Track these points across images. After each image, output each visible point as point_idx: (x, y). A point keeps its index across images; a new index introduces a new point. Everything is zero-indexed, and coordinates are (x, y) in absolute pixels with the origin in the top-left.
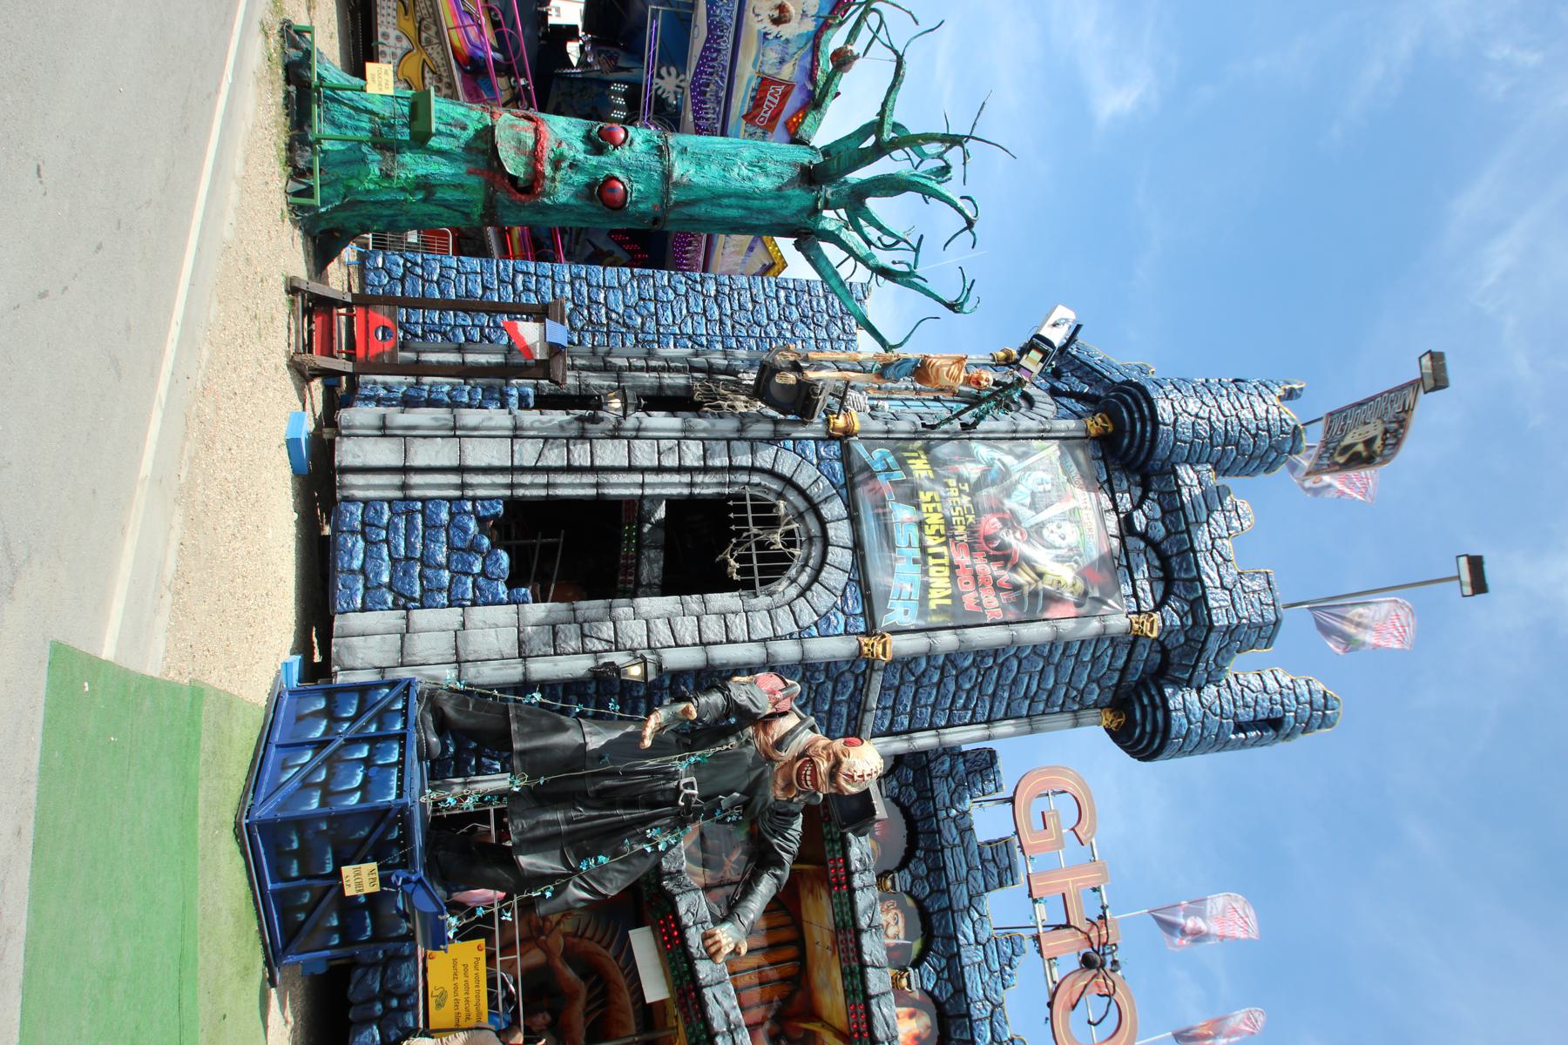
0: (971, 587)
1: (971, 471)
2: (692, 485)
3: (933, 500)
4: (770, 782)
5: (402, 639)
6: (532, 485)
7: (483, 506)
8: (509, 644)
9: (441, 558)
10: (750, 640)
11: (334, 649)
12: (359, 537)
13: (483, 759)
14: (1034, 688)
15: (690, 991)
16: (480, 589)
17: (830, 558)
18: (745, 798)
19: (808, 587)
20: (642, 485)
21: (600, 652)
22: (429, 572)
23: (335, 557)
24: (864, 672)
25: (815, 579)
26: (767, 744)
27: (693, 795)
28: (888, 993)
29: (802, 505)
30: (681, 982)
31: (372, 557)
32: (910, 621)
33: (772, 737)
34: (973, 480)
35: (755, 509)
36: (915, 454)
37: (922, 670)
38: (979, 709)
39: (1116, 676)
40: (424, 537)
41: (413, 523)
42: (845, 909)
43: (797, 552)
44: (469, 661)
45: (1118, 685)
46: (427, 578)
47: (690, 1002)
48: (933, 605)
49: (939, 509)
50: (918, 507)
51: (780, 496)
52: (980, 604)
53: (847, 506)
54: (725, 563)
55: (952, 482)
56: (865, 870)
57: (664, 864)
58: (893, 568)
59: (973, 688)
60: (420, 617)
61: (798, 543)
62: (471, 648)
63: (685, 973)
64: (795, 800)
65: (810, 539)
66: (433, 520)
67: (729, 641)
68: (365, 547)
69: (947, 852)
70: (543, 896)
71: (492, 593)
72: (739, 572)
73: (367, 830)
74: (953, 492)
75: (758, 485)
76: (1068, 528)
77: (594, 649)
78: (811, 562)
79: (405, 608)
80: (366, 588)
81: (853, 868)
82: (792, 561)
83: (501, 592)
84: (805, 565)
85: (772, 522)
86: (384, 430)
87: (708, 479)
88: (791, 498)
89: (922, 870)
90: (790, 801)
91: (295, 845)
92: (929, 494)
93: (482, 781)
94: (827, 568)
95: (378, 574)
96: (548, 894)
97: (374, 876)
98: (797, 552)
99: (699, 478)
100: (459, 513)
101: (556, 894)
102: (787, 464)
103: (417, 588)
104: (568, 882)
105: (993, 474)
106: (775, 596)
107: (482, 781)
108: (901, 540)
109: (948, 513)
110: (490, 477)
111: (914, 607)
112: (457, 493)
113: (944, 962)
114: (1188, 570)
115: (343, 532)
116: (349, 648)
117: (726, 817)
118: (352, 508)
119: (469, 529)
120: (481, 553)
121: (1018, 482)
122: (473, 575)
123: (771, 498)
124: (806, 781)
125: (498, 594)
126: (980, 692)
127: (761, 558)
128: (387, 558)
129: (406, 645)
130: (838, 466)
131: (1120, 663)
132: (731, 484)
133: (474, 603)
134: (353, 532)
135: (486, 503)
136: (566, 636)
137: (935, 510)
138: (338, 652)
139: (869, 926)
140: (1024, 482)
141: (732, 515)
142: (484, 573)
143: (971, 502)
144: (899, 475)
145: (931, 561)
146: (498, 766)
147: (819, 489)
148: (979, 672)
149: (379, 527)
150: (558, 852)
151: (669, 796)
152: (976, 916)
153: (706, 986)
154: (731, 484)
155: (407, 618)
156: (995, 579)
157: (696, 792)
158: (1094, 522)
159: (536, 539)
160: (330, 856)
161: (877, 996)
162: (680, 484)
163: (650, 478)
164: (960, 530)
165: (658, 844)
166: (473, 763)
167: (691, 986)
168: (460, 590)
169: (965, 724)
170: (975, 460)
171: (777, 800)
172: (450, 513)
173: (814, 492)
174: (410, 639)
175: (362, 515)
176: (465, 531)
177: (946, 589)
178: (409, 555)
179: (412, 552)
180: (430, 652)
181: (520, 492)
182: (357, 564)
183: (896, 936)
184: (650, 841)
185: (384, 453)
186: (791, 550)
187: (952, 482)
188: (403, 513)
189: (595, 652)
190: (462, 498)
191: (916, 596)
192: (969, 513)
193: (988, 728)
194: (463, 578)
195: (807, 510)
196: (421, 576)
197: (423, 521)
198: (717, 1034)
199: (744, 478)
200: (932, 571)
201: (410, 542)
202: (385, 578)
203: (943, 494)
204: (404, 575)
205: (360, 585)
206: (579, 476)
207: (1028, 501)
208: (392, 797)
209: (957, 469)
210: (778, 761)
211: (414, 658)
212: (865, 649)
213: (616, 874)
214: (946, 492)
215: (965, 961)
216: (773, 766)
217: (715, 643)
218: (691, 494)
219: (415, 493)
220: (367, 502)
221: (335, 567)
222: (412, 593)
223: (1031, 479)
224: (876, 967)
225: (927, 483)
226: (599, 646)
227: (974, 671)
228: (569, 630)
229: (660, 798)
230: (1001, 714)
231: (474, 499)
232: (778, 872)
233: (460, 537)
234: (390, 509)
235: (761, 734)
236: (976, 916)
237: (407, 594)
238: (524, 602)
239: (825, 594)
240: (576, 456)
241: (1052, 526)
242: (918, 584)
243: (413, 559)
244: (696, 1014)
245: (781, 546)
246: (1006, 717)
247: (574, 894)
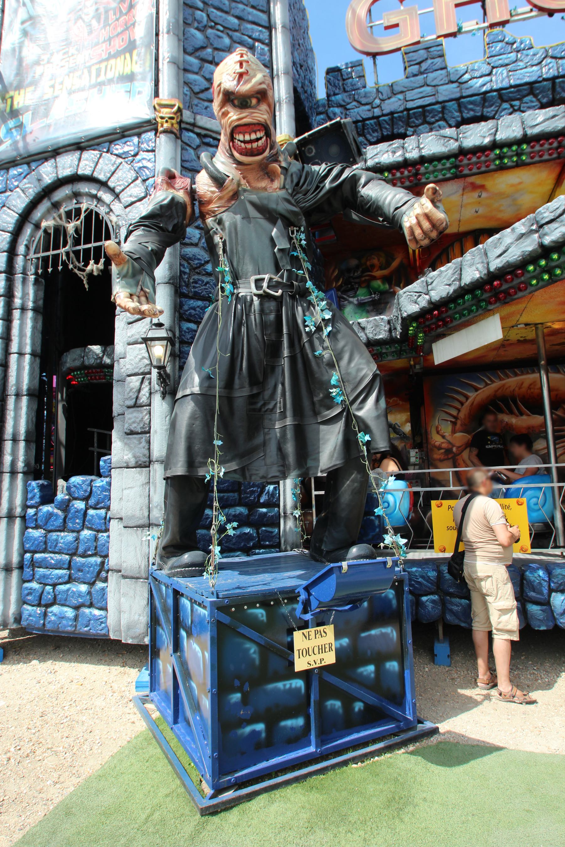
2: (23, 309)
4: (264, 194)
5: (124, 577)
6: (14, 453)
7: (32, 499)
8: (137, 476)
9: (69, 537)
11: (130, 641)
12: (49, 610)
13: (262, 500)
15: (493, 288)
16: (98, 503)
17: (88, 172)
18: (279, 222)
19: (112, 190)
20: (21, 354)
21: (150, 389)
22: (81, 550)
23: (63, 632)
24: (198, 135)
25: (103, 184)
26: (220, 198)
27: (271, 279)
28: (522, 118)
29: (45, 205)
30: (483, 300)
31: (66, 600)
33: (213, 192)
35: (46, 249)
37: (202, 80)
38: (256, 35)
40: (54, 553)
41: (41, 562)
42: (440, 167)
43: (84, 207)
44: (149, 515)
46: (85, 551)
47: (505, 287)
51: (37, 226)
53: (46, 159)
54: (90, 275)
56: (403, 148)
57: (381, 337)
59: (230, 37)
60: (113, 561)
61: (77, 206)
62: (138, 513)
63: (474, 297)
64: (284, 164)
65: (76, 195)
66: (38, 545)
68: (59, 604)
69: (410, 105)
70: (368, 443)
71: (102, 491)
72: (97, 262)
73: (248, 645)
75: (27, 247)
77: (148, 395)
78: (94, 192)
80: (91, 605)
81: (401, 159)
82: (92, 211)
83: (101, 484)
84: (95, 197)
85: (59, 231)
87: (18, 293)
88: (39, 215)
90: (285, 170)
91: (260, 727)
93: (285, 502)
94: (96, 175)
95: (80, 595)
96: (367, 438)
97: (312, 634)
98: (84, 207)
99: (18, 302)
100: (36, 520)
101: (367, 429)
103: (93, 560)
104: (356, 416)
106: (120, 223)
107: (285, 502)
110: (3, 493)
112: (18, 521)
113: (505, 105)
115: (44, 624)
116: (129, 628)
117: (301, 246)
118: (25, 615)
119: (48, 511)
120: (69, 501)
122: (87, 509)
123: (40, 233)
124: (251, 141)
125: (102, 487)
126: (236, 31)
127: (87, 241)
128: (68, 586)
129: (130, 574)
130: (14, 172)
132: (24, 273)
133: (108, 508)
134: (45, 614)
135: (30, 496)
136: (134, 422)
138: (132, 638)
139: (457, 140)
141: (50, 270)
142: (86, 499)
146: (271, 487)
147: (30, 188)
148: (211, 27)
149: (42, 592)
150: (322, 427)
151: (272, 305)
152: (467, 76)
153: (488, 269)
154: (24, 273)
157: (267, 277)
159: (93, 452)
160: (280, 685)
161: (524, 129)
162: (22, 319)
163: (14, 347)
165: (323, 320)
166: (264, 510)
167: (488, 287)
168: (98, 521)
169: (271, 51)
171: (284, 187)
172: (37, 527)
173: (32, 192)
174: (126, 570)
175: (33, 606)
176: (50, 515)
177: (125, 58)
178: (66, 566)
179: (64, 564)
180: (138, 552)
181: (20, 465)
182: (70, 613)
184: (319, 329)
186: (83, 210)
188: (33, 570)
189: (151, 394)
190: (23, 518)
193: (276, 29)
194: (88, 517)
195: (49, 199)
196: (84, 556)
197: (41, 552)
198: (541, 246)
199: (20, 261)
201: (55, 564)
202: (84, 588)
204: (82, 571)
205: (87, 611)
206: (8, 412)
210: (239, 185)
211: (143, 567)
212: (165, 125)
213: (353, 365)
215: (505, 84)
216: (245, 191)
218: (35, 310)
219: (15, 559)
220: (22, 601)
221: (73, 633)
222: (96, 565)
224: (497, 131)
226: (145, 391)
227: (210, 31)
228: (130, 419)
229: (272, 317)
230: (264, 17)
231: (25, 507)
232: (363, 181)
233: (55, 520)
234: (29, 581)
235: (212, 206)
236: (467, 76)
237: (97, 568)
239: (119, 174)
243: (70, 562)
244: (517, 276)
246: (268, 12)
247: (369, 410)
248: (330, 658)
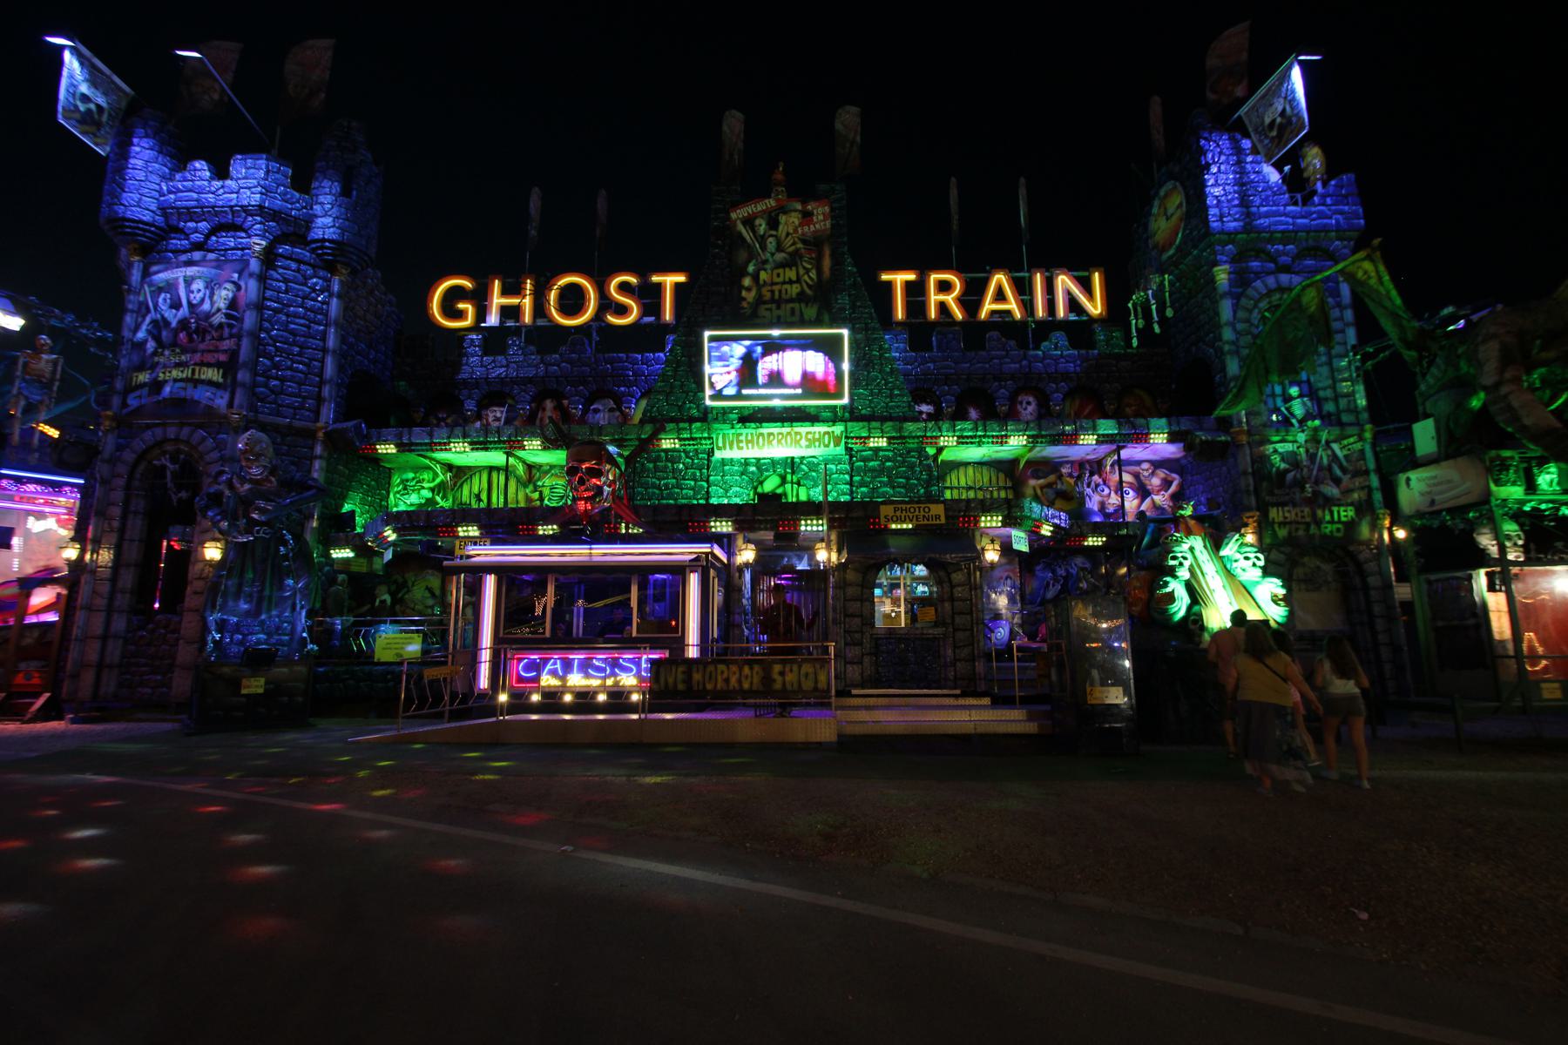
1: (151, 345)
3: (164, 373)
14: (302, 321)
32: (227, 396)
39: (303, 267)
45: (314, 266)
48: (221, 380)
50: (166, 382)
52: (226, 351)
86: (75, 676)
89: (465, 392)
92: (161, 375)
105: (155, 332)
108: (183, 394)
111: (219, 393)
114: (225, 212)
121: (163, 316)
131: (294, 265)
143: (168, 348)
144: (145, 391)
145: (196, 376)
170: (145, 342)
183: (502, 412)
185: (88, 677)
187: (156, 359)
191: (214, 390)
200: (203, 377)
223: (163, 307)
225: (154, 375)
242: (207, 388)
248: (261, 691)
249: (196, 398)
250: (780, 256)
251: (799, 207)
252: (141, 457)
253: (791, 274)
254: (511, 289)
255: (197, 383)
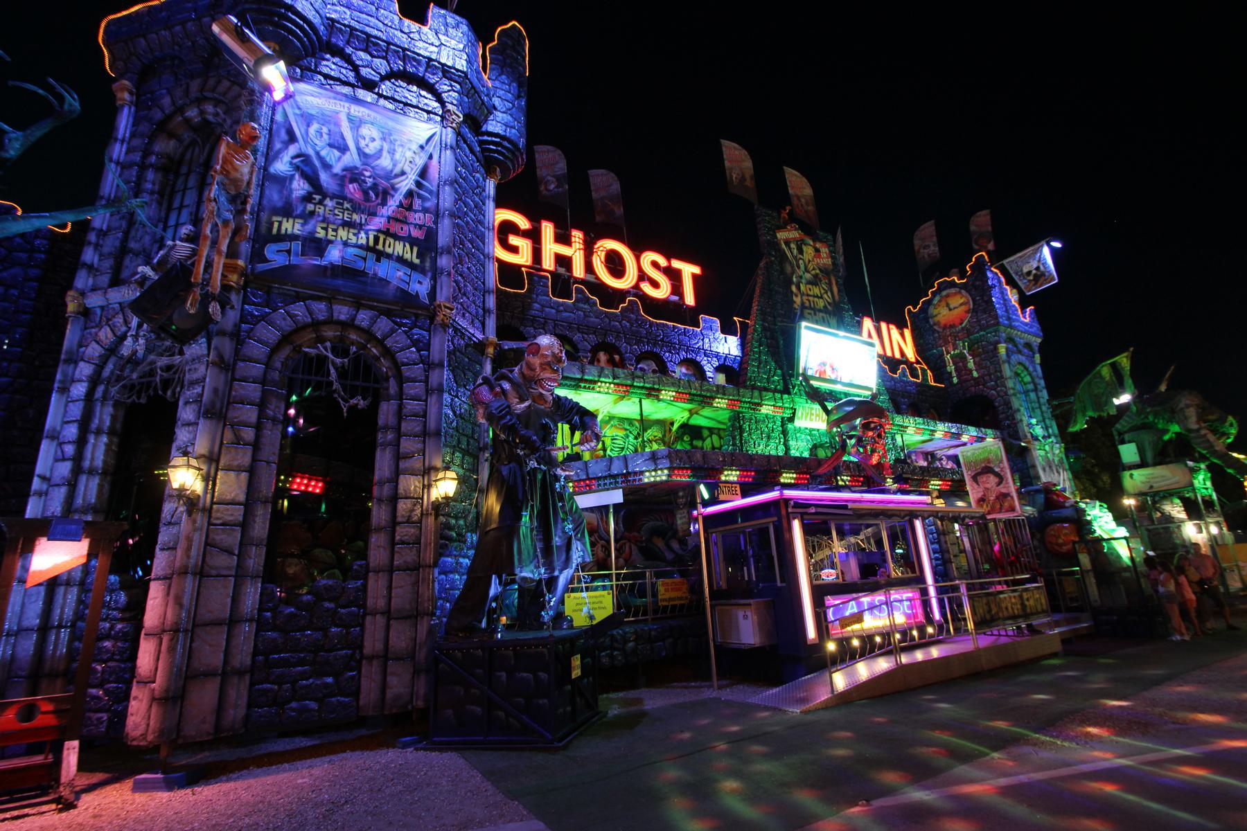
0: (406, 228)
3: (326, 229)
10: (426, 401)
34: (311, 189)
36: (276, 225)
48: (417, 261)
49: (335, 227)
50: (331, 242)
52: (420, 227)
54: (353, 409)
55: (310, 207)
58: (381, 279)
62: (408, 607)
67: (425, 416)
74: (320, 210)
76: (365, 131)
79: (359, 662)
92: (319, 230)
95: (326, 685)
102: (269, 333)
108: (361, 265)
109: (340, 222)
111: (416, 276)
114: (419, 62)
121: (318, 154)
133: (364, 606)
136: (406, 535)
137: (335, 230)
140: (318, 149)
143: (332, 199)
145: (380, 247)
155: (371, 658)
156: (401, 205)
158: (362, 109)
164: (355, 217)
182: (313, 705)
187: (310, 207)
191: (409, 271)
192: (342, 204)
200: (389, 251)
203: (321, 218)
207: (337, 153)
208: (545, 651)
209: (297, 198)
214: (319, 215)
217: (425, 426)
223: (317, 142)
225: (309, 227)
238: (368, 565)
240: (231, 518)
241: (362, 143)
242: (398, 265)
245: (346, 360)
249: (381, 274)
250: (808, 276)
251: (812, 243)
252: (286, 339)
253: (816, 291)
254: (563, 238)
255: (380, 255)
